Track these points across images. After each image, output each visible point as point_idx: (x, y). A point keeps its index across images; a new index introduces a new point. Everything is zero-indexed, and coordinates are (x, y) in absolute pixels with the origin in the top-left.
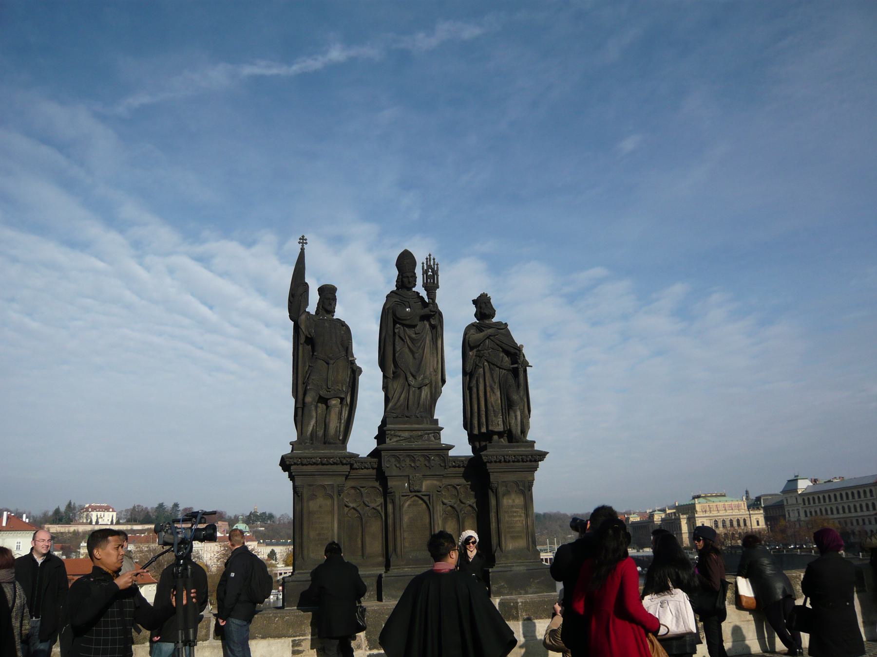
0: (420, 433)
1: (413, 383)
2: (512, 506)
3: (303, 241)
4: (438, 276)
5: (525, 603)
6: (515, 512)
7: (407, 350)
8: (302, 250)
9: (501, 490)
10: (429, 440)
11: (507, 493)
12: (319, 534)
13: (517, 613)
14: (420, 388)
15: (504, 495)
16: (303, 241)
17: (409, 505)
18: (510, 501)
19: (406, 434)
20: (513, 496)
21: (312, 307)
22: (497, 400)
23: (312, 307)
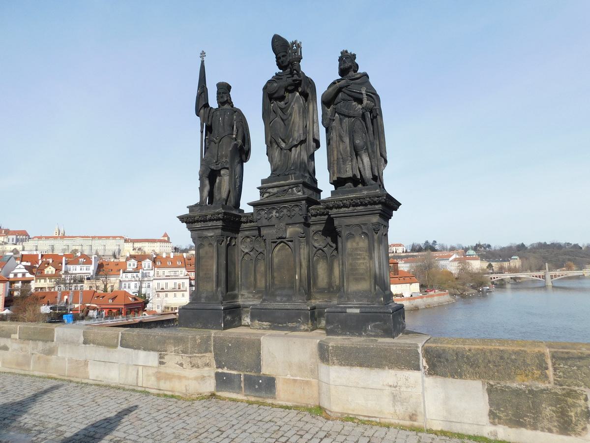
0: (286, 188)
1: (283, 145)
2: (356, 249)
3: (203, 54)
4: (301, 49)
5: (336, 348)
6: (359, 255)
7: (278, 119)
8: (203, 62)
9: (344, 233)
10: (292, 193)
11: (351, 236)
12: (206, 274)
13: (328, 357)
14: (290, 150)
15: (347, 239)
16: (203, 54)
17: (279, 250)
18: (354, 244)
19: (276, 190)
20: (357, 239)
21: (213, 103)
22: (346, 148)
23: (213, 103)
